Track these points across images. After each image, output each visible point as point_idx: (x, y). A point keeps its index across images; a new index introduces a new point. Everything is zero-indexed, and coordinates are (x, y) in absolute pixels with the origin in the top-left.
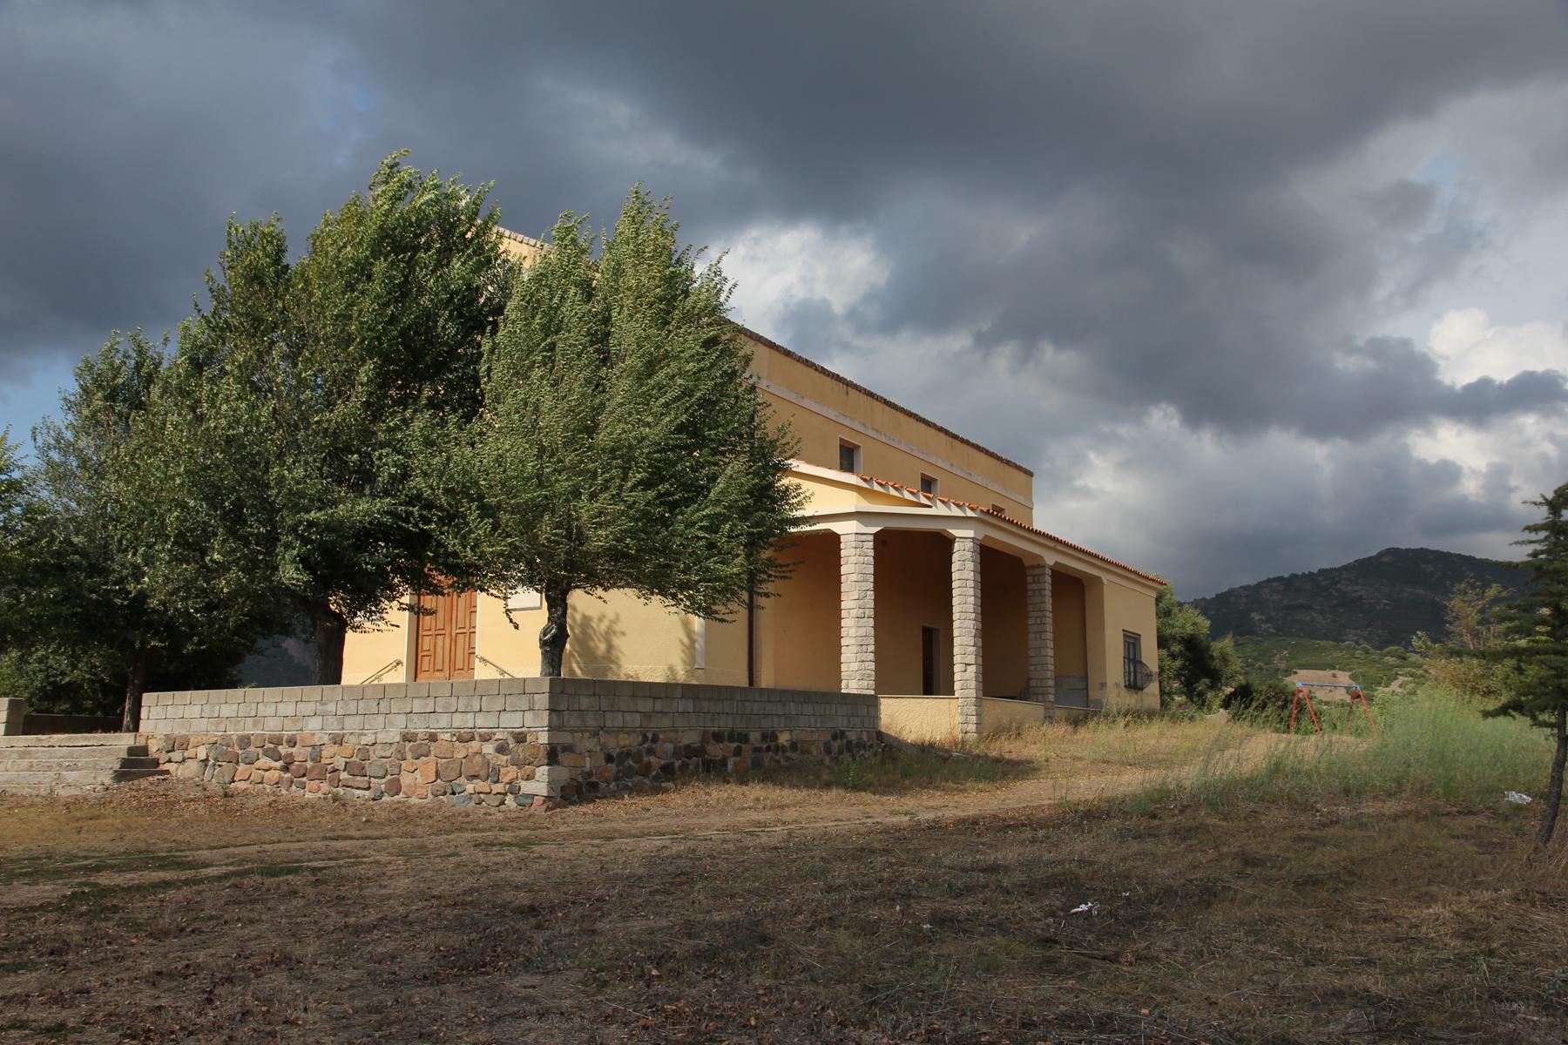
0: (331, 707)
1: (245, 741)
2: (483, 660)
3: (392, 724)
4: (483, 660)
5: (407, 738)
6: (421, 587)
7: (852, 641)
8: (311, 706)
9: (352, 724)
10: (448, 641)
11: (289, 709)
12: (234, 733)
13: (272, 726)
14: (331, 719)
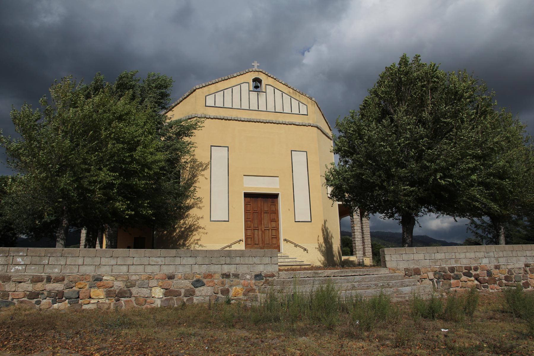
0: (491, 254)
1: (452, 270)
2: (285, 240)
3: (519, 260)
4: (285, 240)
5: (527, 265)
6: (180, 208)
7: (359, 239)
8: (482, 254)
9: (502, 261)
10: (260, 232)
11: (472, 255)
12: (446, 266)
13: (465, 263)
14: (493, 259)
